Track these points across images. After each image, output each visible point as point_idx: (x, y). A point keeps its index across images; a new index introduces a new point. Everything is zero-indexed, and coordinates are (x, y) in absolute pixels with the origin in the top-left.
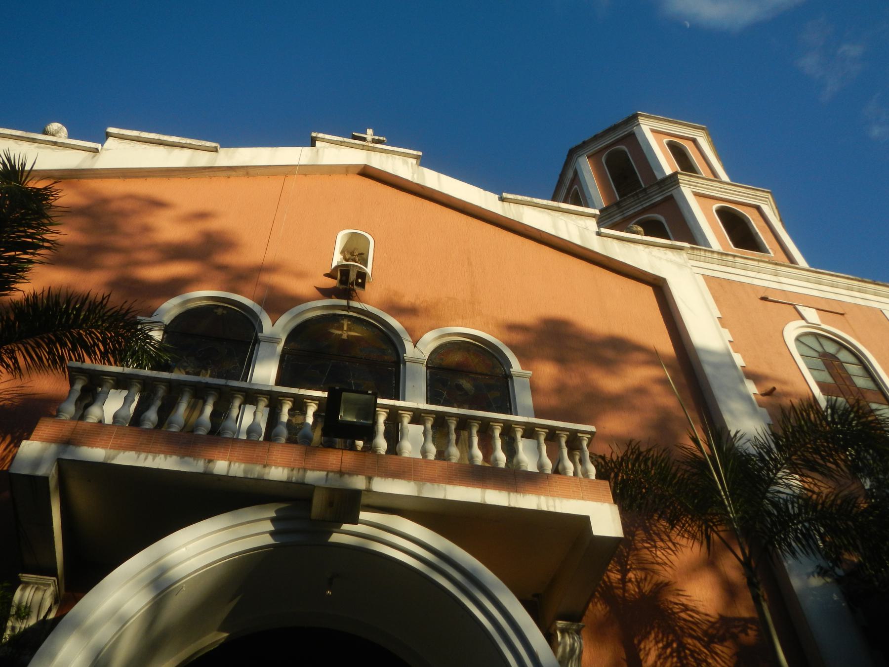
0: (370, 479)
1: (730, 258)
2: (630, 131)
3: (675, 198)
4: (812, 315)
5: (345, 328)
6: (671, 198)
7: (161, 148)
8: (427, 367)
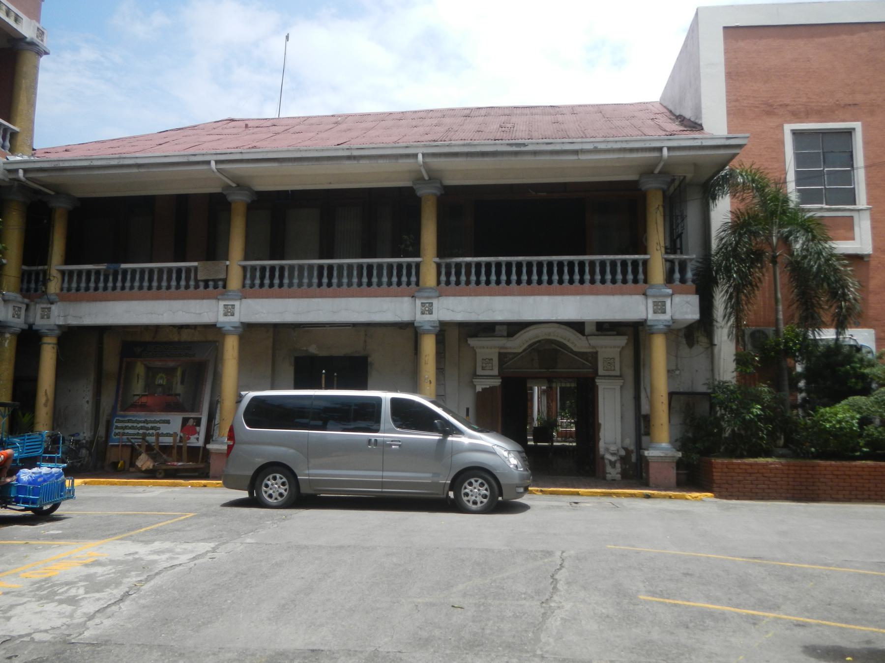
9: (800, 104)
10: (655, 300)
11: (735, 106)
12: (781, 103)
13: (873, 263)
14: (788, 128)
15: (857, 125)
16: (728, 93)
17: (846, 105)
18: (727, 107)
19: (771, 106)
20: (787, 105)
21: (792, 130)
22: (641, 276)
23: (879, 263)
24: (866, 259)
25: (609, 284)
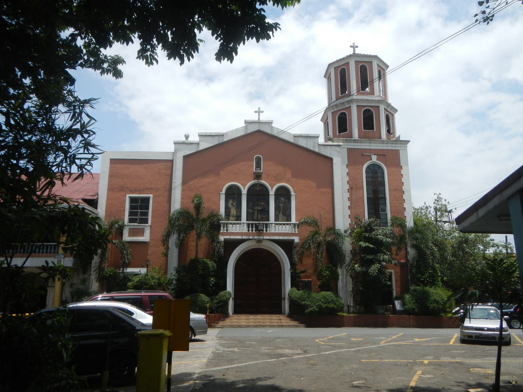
0: (263, 237)
1: (357, 141)
2: (348, 61)
3: (351, 107)
4: (374, 158)
5: (258, 187)
6: (350, 107)
7: (211, 137)
8: (275, 195)
9: (133, 188)
10: (58, 259)
11: (111, 187)
12: (127, 187)
13: (150, 244)
14: (128, 196)
15: (151, 196)
16: (109, 182)
17: (148, 188)
18: (108, 188)
19: (123, 188)
20: (129, 188)
21: (129, 197)
22: (56, 251)
23: (153, 244)
24: (148, 243)
25: (41, 254)
